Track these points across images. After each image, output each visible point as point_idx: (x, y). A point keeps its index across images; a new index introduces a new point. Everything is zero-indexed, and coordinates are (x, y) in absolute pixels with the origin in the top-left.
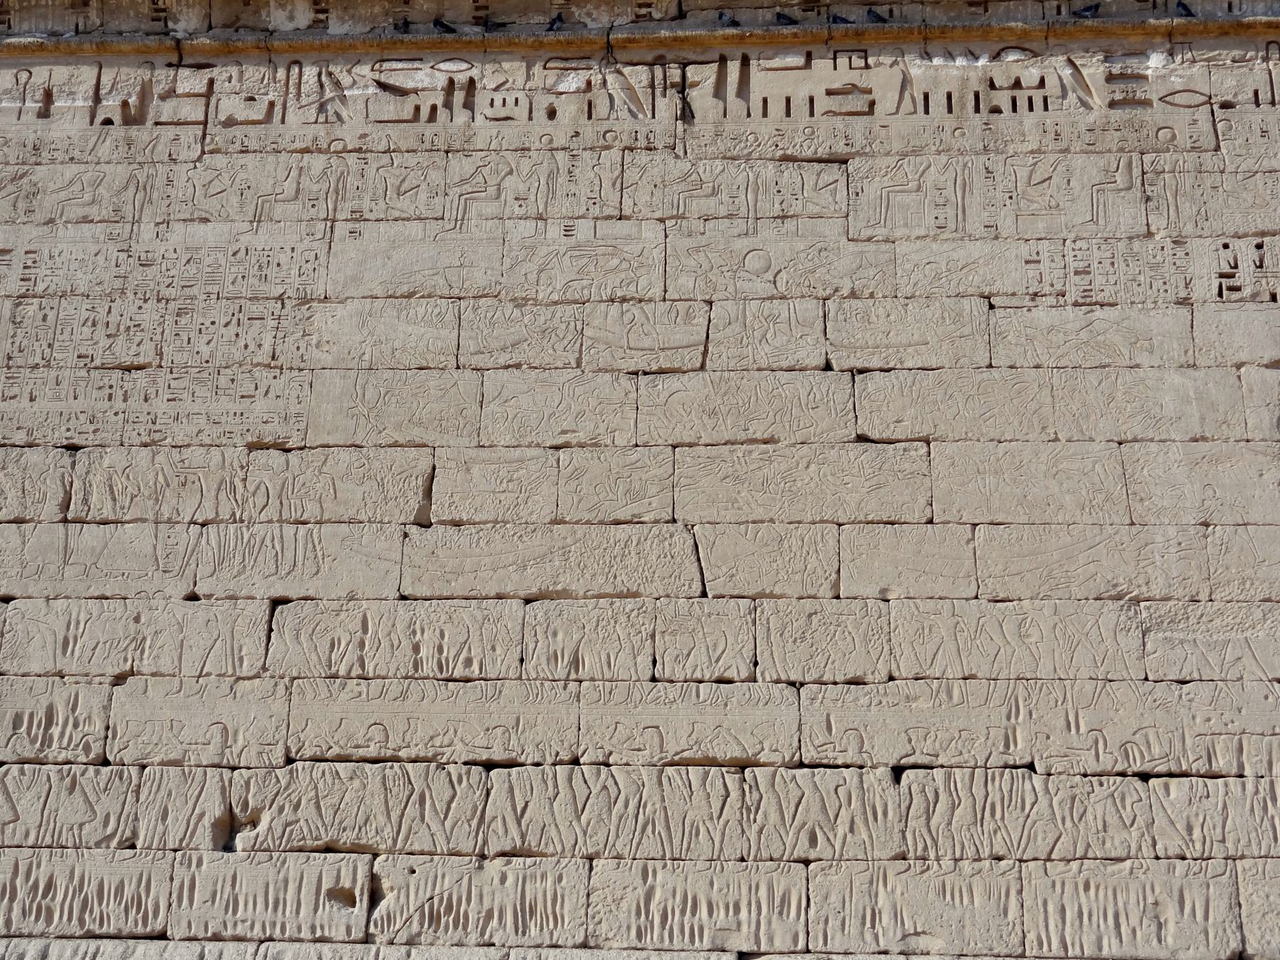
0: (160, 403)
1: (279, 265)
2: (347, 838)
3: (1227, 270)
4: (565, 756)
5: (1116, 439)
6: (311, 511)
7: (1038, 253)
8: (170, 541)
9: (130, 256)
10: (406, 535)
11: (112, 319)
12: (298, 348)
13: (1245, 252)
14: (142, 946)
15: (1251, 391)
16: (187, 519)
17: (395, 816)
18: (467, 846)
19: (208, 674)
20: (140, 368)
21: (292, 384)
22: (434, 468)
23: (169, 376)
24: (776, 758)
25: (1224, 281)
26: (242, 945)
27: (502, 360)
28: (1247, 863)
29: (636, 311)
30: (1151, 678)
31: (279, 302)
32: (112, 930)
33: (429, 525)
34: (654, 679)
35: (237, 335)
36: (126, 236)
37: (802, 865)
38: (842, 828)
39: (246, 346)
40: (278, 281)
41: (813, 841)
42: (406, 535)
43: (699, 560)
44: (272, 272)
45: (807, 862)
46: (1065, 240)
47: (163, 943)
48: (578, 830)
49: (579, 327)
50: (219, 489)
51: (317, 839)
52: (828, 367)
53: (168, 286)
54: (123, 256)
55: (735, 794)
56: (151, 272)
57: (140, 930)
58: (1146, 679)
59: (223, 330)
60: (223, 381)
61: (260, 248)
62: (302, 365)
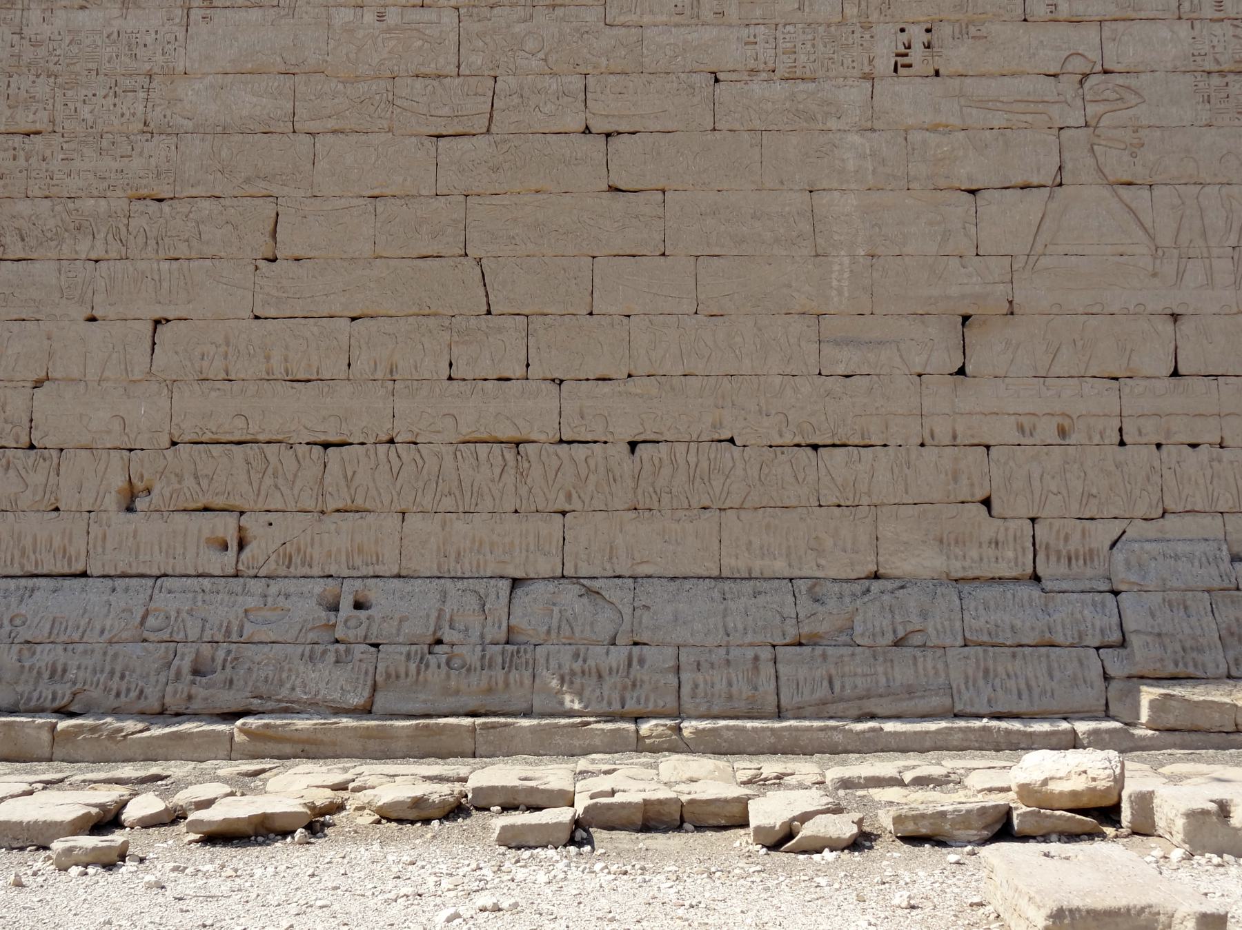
0: (55, 162)
1: (145, 46)
2: (219, 502)
3: (902, 50)
4: (386, 438)
5: (808, 188)
6: (182, 250)
7: (755, 36)
8: (70, 275)
9: (22, 38)
10: (257, 268)
11: (10, 91)
12: (165, 116)
13: (917, 35)
14: (67, 582)
15: (913, 149)
16: (84, 256)
17: (255, 486)
18: (309, 504)
19: (107, 380)
20: (37, 133)
21: (161, 146)
22: (277, 215)
23: (62, 140)
24: (543, 437)
25: (899, 59)
26: (143, 581)
27: (331, 124)
28: (884, 509)
29: (436, 83)
30: (823, 373)
31: (148, 77)
32: (45, 571)
33: (274, 260)
34: (450, 378)
35: (115, 105)
36: (17, 20)
37: (560, 515)
38: (591, 487)
39: (123, 115)
40: (146, 59)
41: (569, 497)
42: (257, 268)
43: (485, 285)
44: (140, 52)
45: (564, 513)
46: (777, 25)
47: (83, 580)
48: (394, 493)
49: (390, 98)
50: (108, 233)
51: (196, 502)
52: (587, 130)
53: (55, 64)
54: (16, 37)
55: (512, 463)
56: (42, 52)
57: (66, 570)
58: (820, 374)
59: (104, 102)
60: (105, 143)
61: (129, 31)
62: (169, 130)
